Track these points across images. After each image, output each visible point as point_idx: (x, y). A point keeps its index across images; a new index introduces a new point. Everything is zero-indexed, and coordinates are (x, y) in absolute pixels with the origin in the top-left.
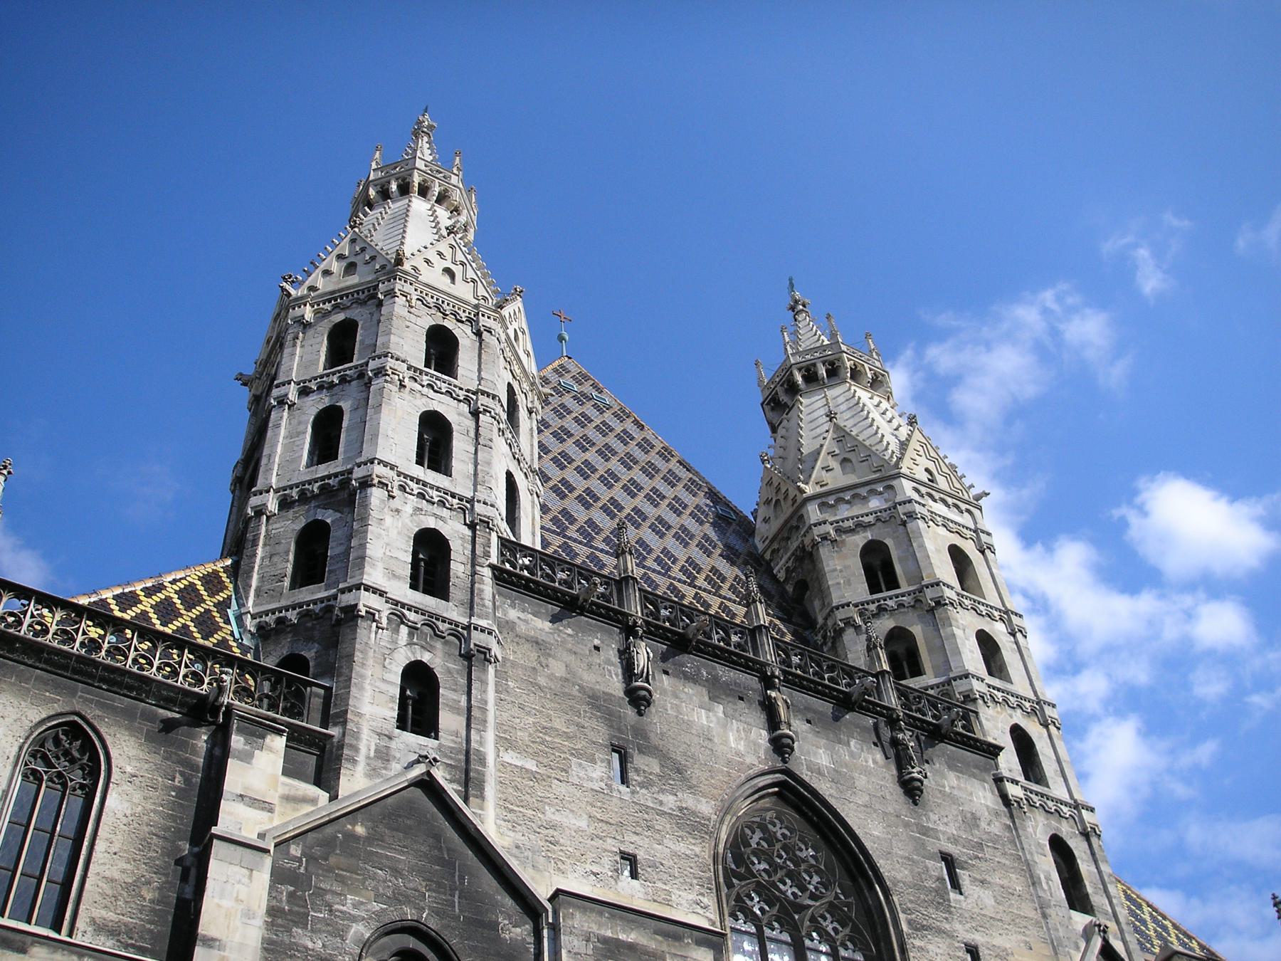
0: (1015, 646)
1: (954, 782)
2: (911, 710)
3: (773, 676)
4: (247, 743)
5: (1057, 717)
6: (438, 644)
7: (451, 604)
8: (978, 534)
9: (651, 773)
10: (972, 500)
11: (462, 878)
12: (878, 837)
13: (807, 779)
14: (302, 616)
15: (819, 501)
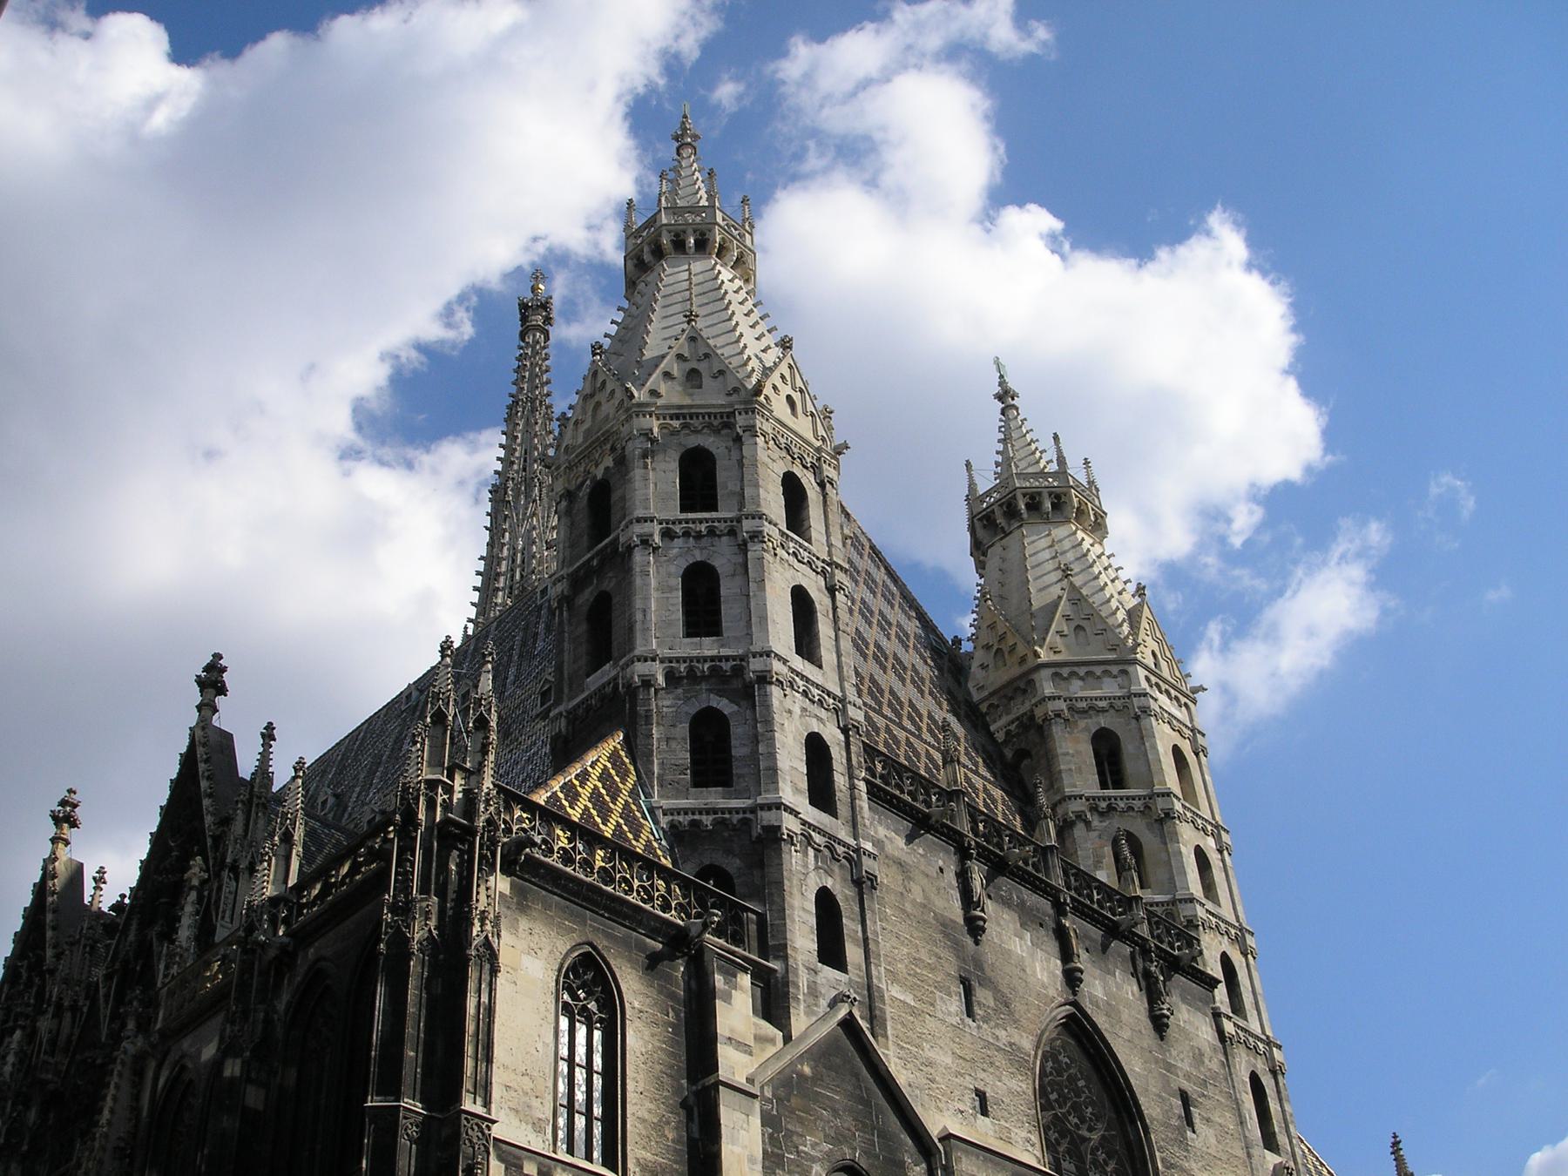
0: (1221, 865)
1: (1186, 1016)
2: (1162, 942)
3: (1065, 903)
4: (726, 983)
5: (1254, 946)
6: (836, 867)
7: (839, 822)
8: (1194, 734)
9: (988, 1007)
10: (1189, 693)
11: (877, 1118)
12: (1138, 1073)
13: (1089, 1012)
14: (716, 823)
15: (1053, 670)
